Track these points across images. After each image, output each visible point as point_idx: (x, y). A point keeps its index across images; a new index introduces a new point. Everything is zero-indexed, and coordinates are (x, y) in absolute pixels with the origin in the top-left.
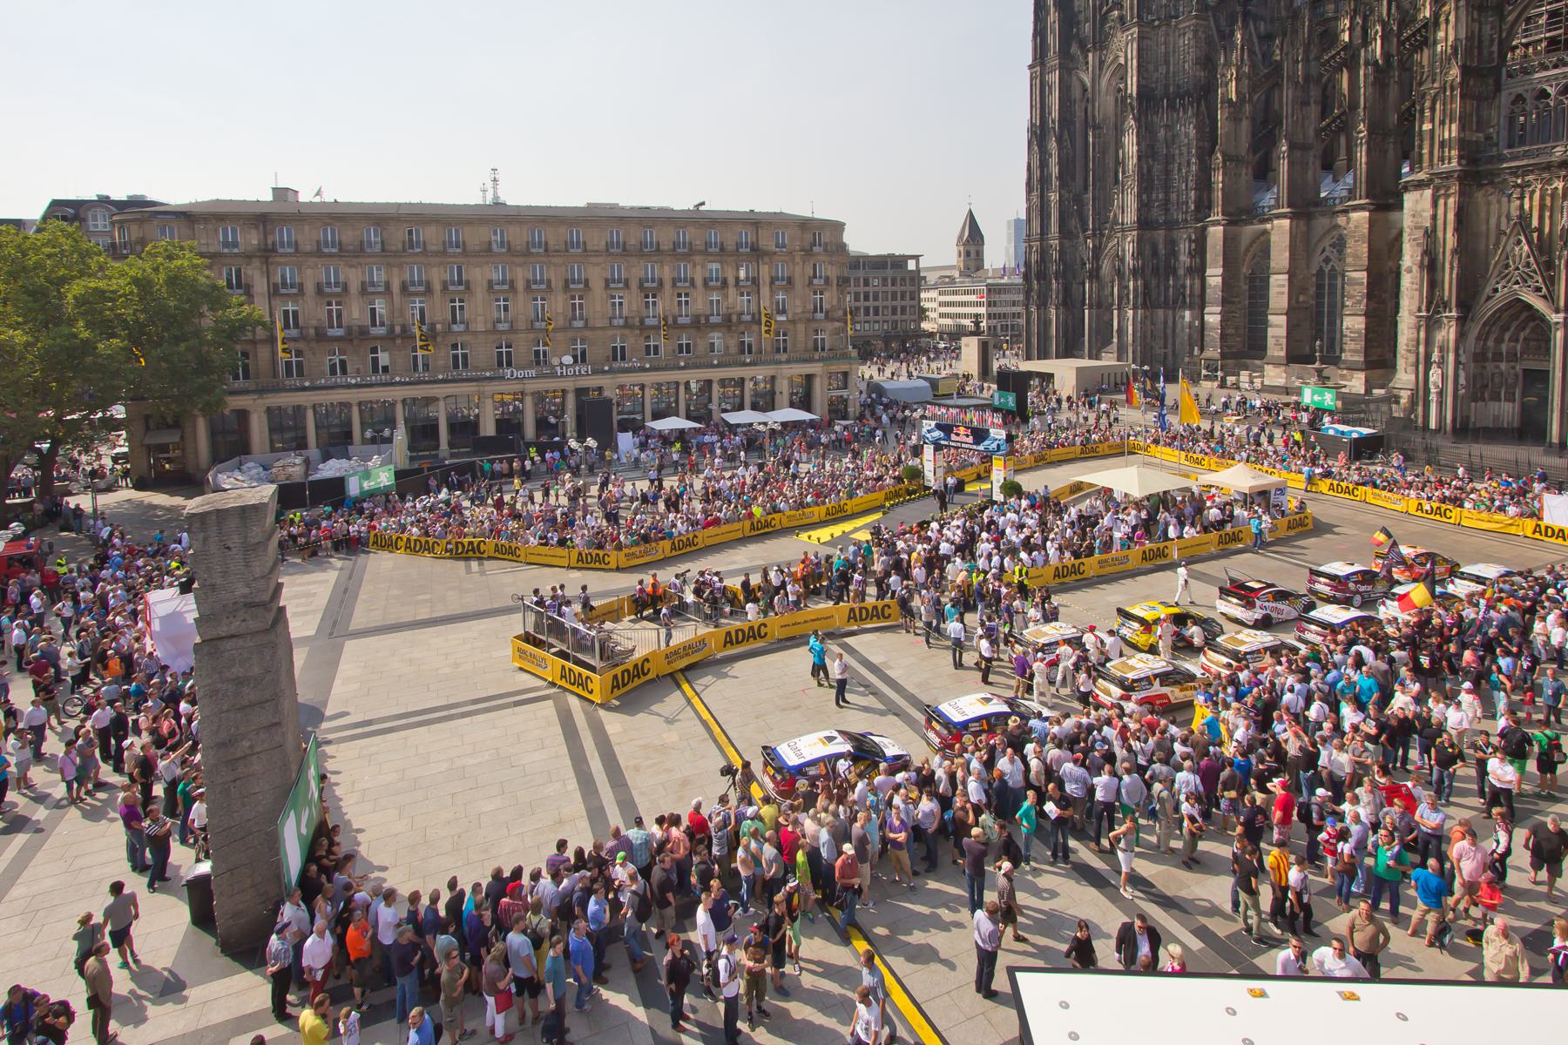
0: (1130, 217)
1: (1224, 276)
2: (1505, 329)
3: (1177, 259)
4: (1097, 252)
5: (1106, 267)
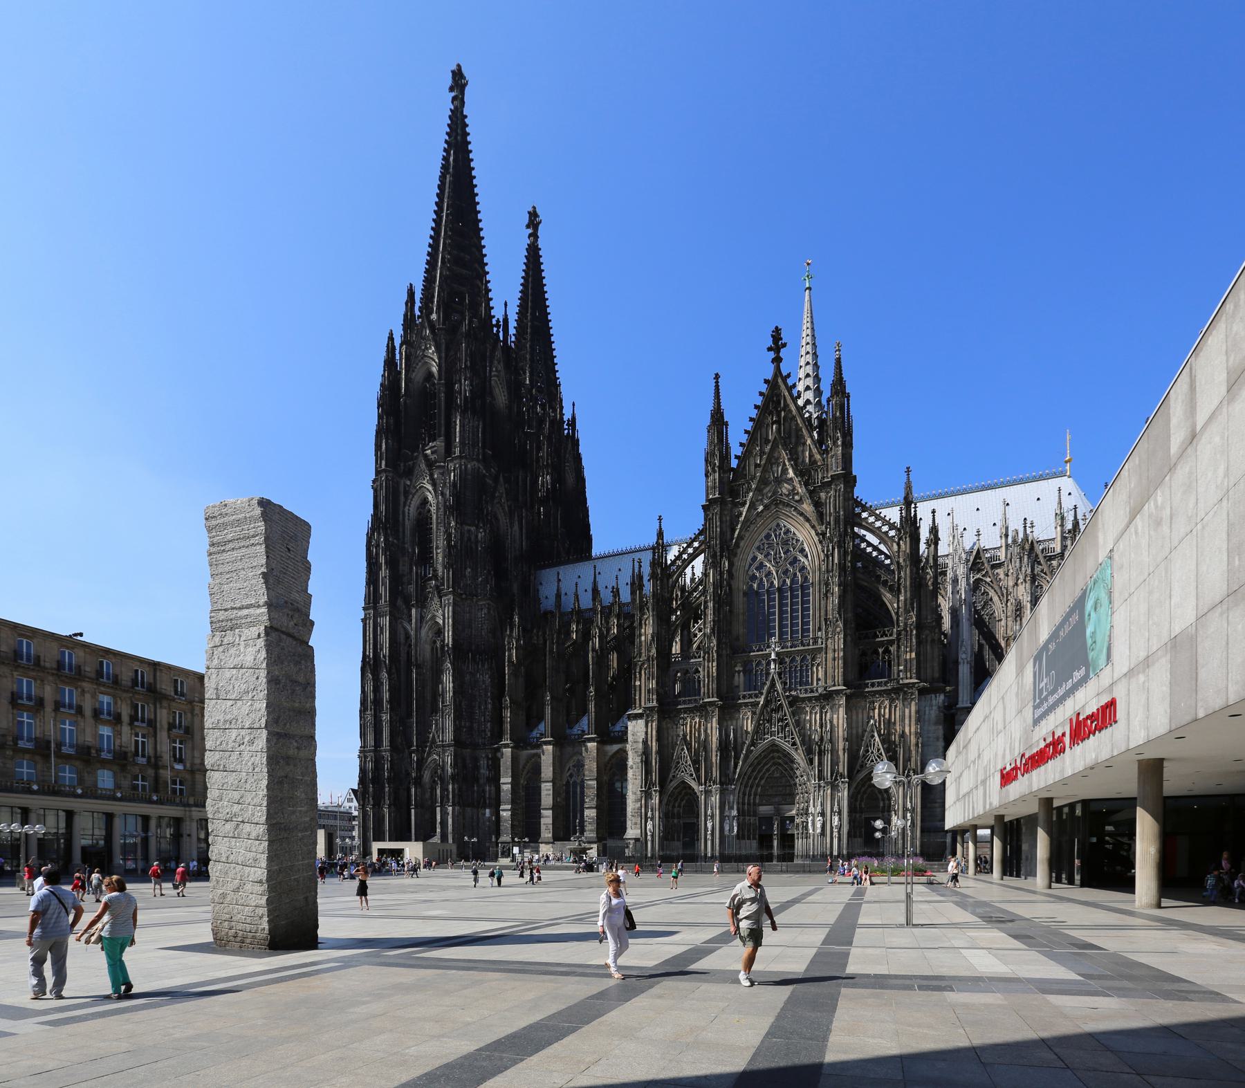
0: (449, 736)
1: (512, 784)
2: (676, 800)
4: (421, 762)
5: (427, 776)
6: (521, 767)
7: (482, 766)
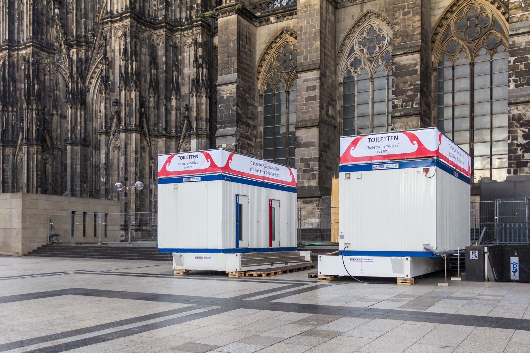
3: (180, 72)
6: (258, 57)
7: (186, 62)
